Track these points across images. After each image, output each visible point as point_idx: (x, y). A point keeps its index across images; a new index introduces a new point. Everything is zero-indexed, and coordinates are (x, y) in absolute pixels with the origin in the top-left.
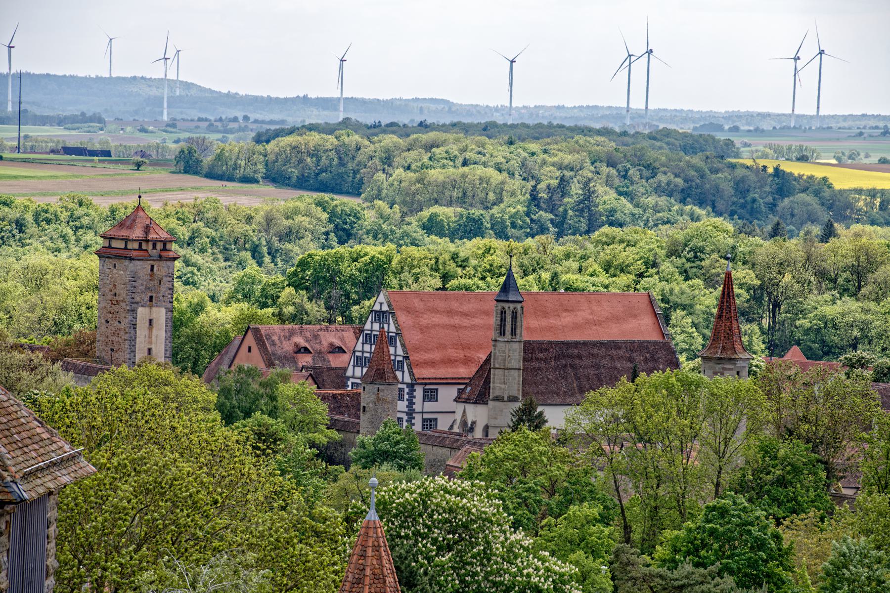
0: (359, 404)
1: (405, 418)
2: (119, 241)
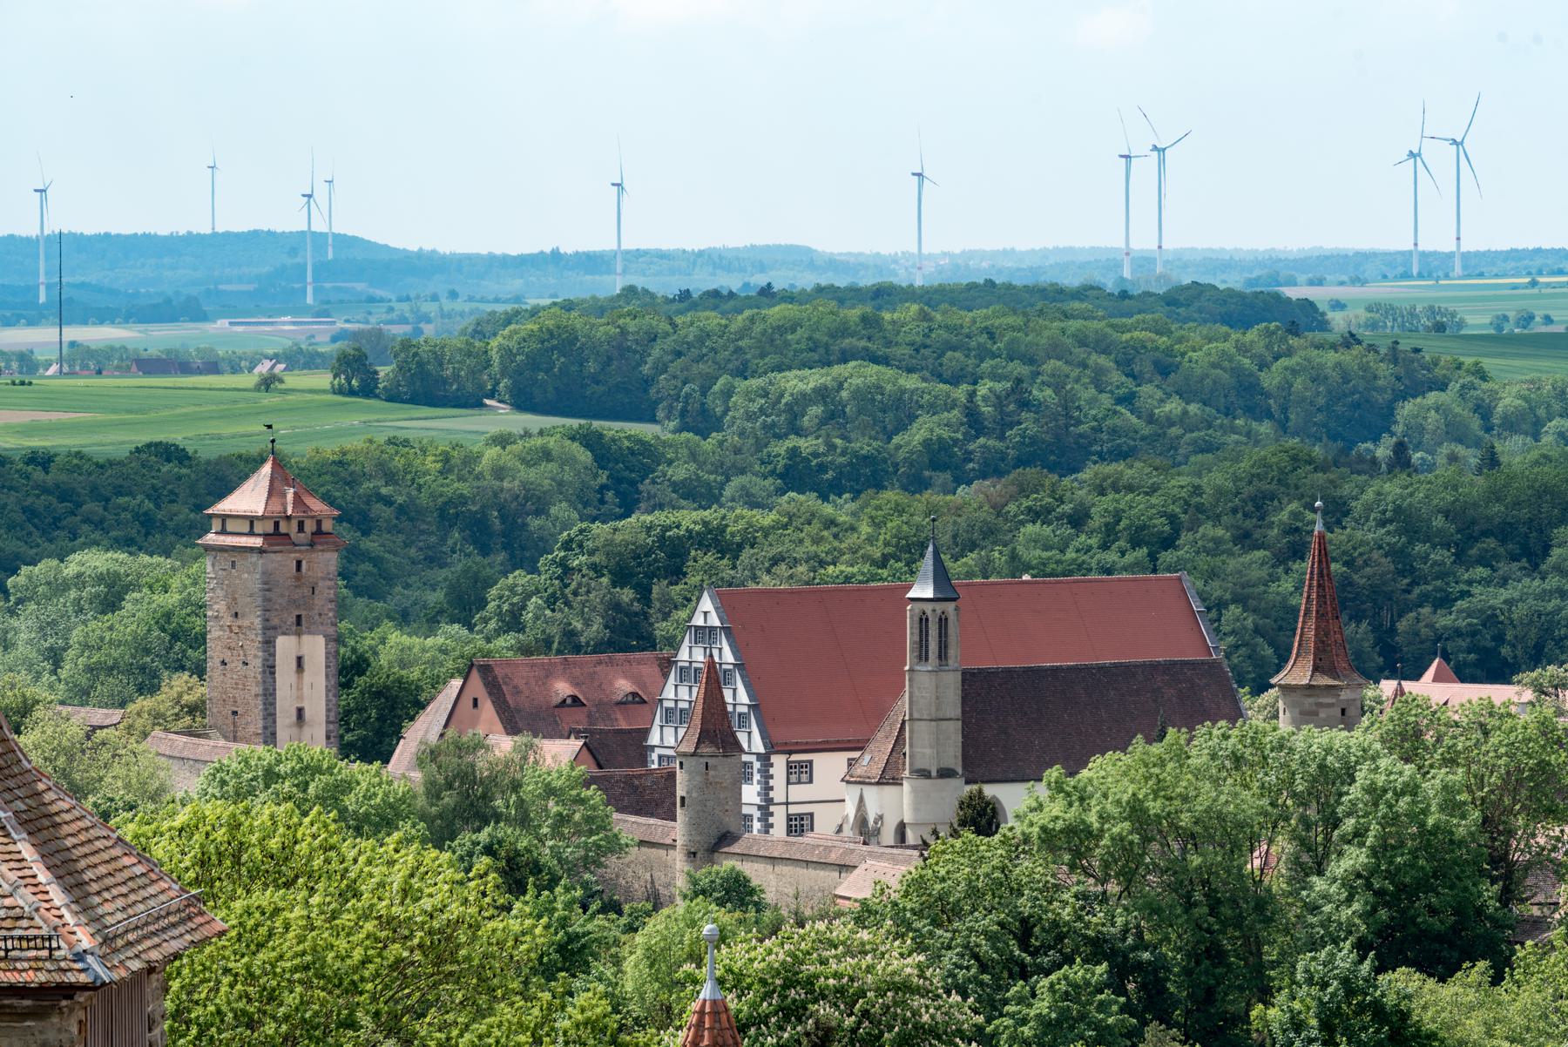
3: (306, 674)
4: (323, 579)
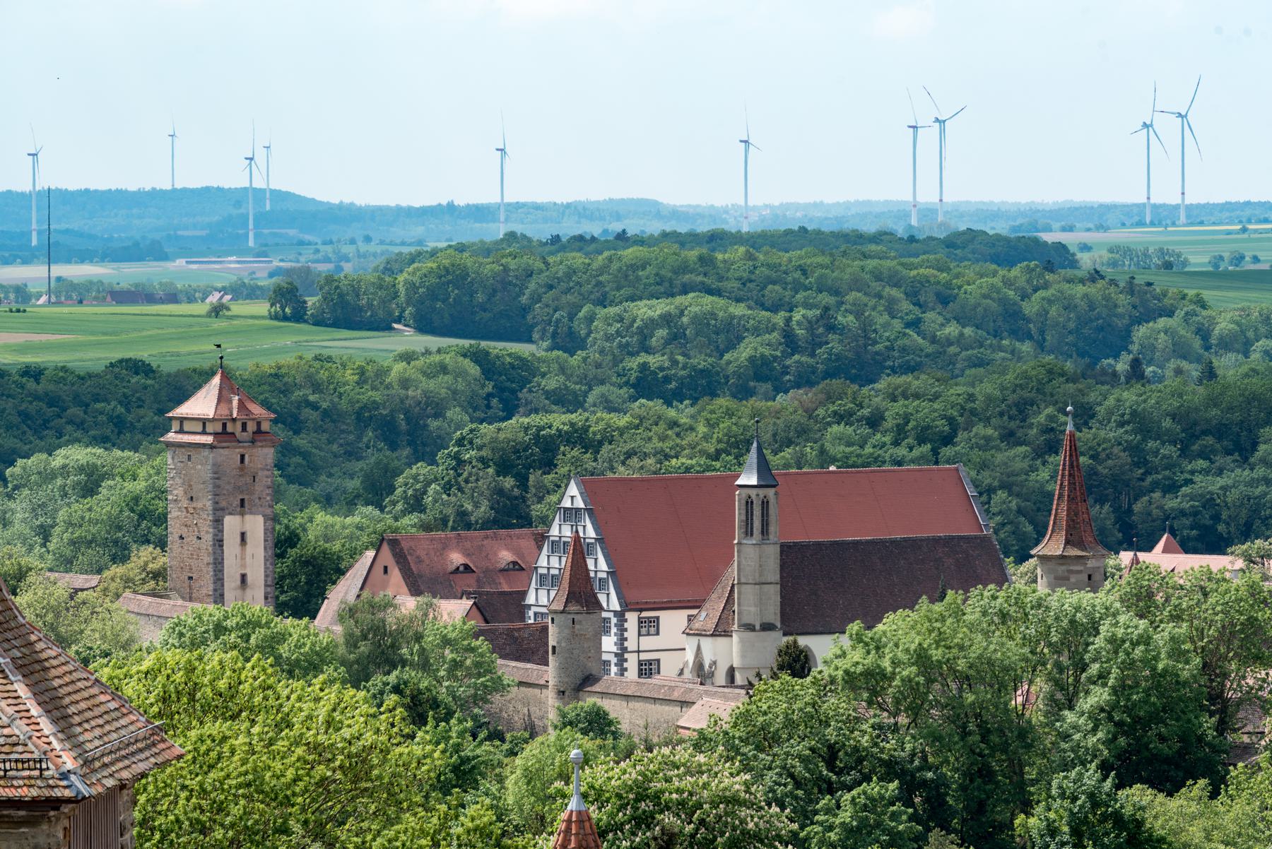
0: (547, 644)
1: (614, 660)
2: (194, 423)
3: (248, 547)
4: (262, 469)
